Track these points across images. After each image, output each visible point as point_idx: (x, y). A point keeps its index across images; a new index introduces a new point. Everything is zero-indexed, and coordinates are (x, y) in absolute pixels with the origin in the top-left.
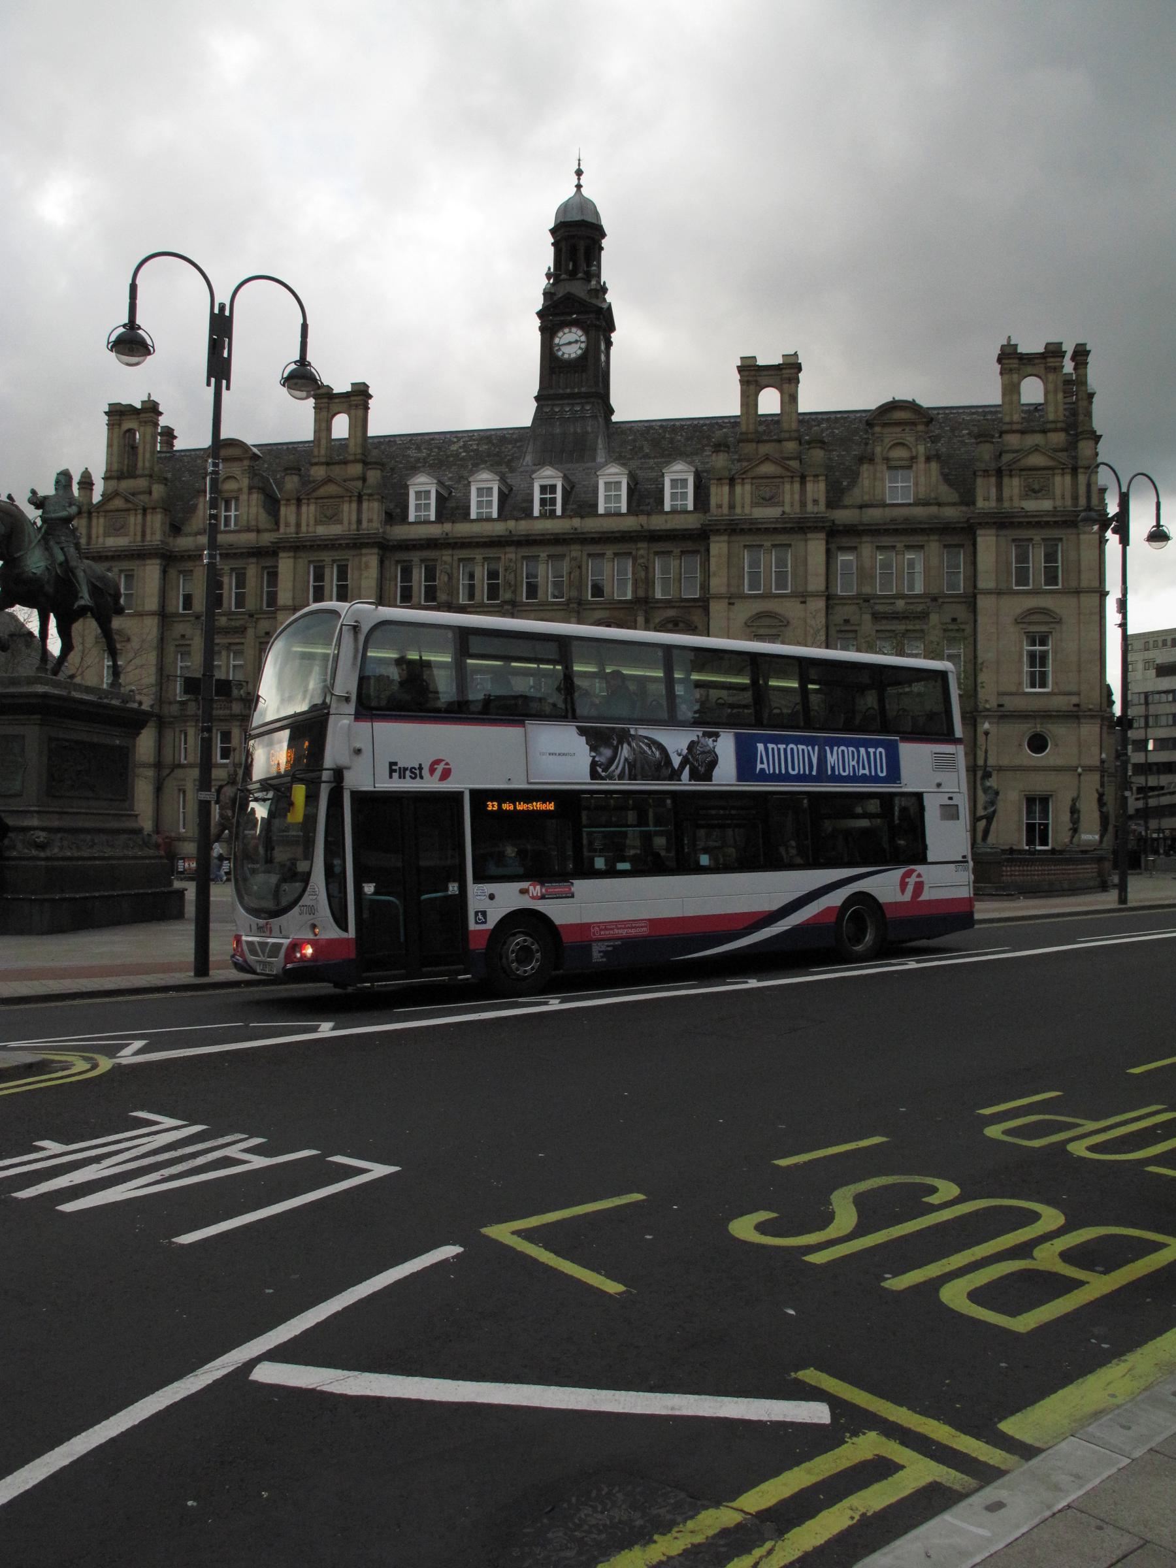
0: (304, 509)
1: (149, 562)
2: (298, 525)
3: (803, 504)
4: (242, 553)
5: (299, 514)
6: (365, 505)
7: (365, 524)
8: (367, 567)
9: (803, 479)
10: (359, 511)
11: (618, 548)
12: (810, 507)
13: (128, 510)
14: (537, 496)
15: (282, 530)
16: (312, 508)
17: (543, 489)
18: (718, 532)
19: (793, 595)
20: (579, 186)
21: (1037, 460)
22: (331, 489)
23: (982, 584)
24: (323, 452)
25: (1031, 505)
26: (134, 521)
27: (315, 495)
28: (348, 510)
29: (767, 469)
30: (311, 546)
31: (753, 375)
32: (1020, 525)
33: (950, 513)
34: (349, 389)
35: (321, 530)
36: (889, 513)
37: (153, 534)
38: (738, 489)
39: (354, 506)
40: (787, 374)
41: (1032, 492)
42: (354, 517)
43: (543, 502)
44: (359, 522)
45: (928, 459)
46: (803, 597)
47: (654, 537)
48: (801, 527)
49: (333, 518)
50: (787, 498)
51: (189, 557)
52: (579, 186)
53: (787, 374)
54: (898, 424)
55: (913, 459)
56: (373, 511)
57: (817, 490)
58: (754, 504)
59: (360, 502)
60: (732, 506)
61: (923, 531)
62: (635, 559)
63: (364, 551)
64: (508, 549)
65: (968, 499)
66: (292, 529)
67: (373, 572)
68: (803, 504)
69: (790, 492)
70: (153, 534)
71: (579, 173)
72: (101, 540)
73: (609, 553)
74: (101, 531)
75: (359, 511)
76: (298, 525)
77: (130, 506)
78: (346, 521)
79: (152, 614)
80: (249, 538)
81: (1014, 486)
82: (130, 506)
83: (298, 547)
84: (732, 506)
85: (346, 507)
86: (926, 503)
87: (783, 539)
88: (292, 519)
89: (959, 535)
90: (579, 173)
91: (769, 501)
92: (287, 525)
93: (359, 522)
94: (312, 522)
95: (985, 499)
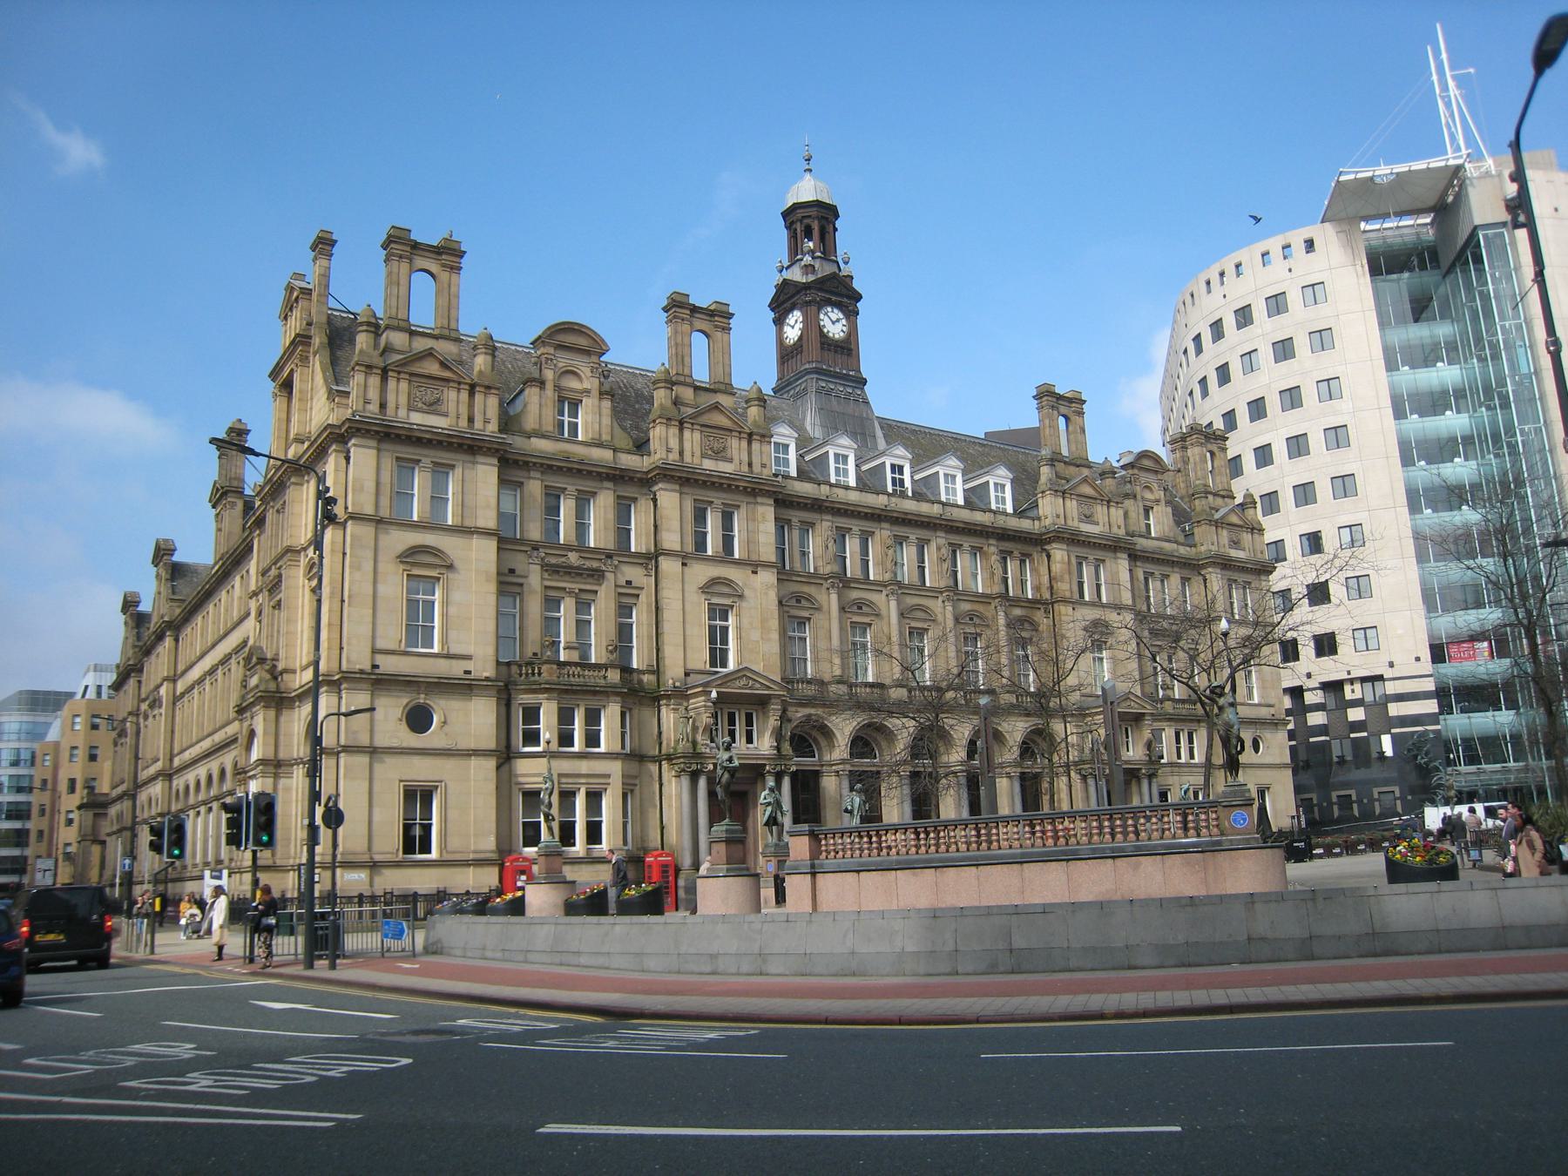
0: (687, 434)
1: (480, 459)
2: (681, 453)
4: (599, 474)
8: (764, 519)
13: (447, 380)
14: (889, 475)
26: (454, 399)
27: (705, 419)
30: (705, 482)
37: (486, 421)
38: (1068, 502)
39: (744, 444)
43: (894, 479)
48: (1113, 546)
49: (719, 454)
51: (526, 463)
58: (1081, 521)
63: (759, 500)
64: (884, 525)
67: (770, 526)
70: (486, 421)
72: (402, 413)
74: (403, 400)
76: (681, 453)
77: (447, 374)
78: (736, 458)
79: (486, 533)
80: (605, 455)
82: (447, 374)
83: (684, 478)
94: (698, 453)
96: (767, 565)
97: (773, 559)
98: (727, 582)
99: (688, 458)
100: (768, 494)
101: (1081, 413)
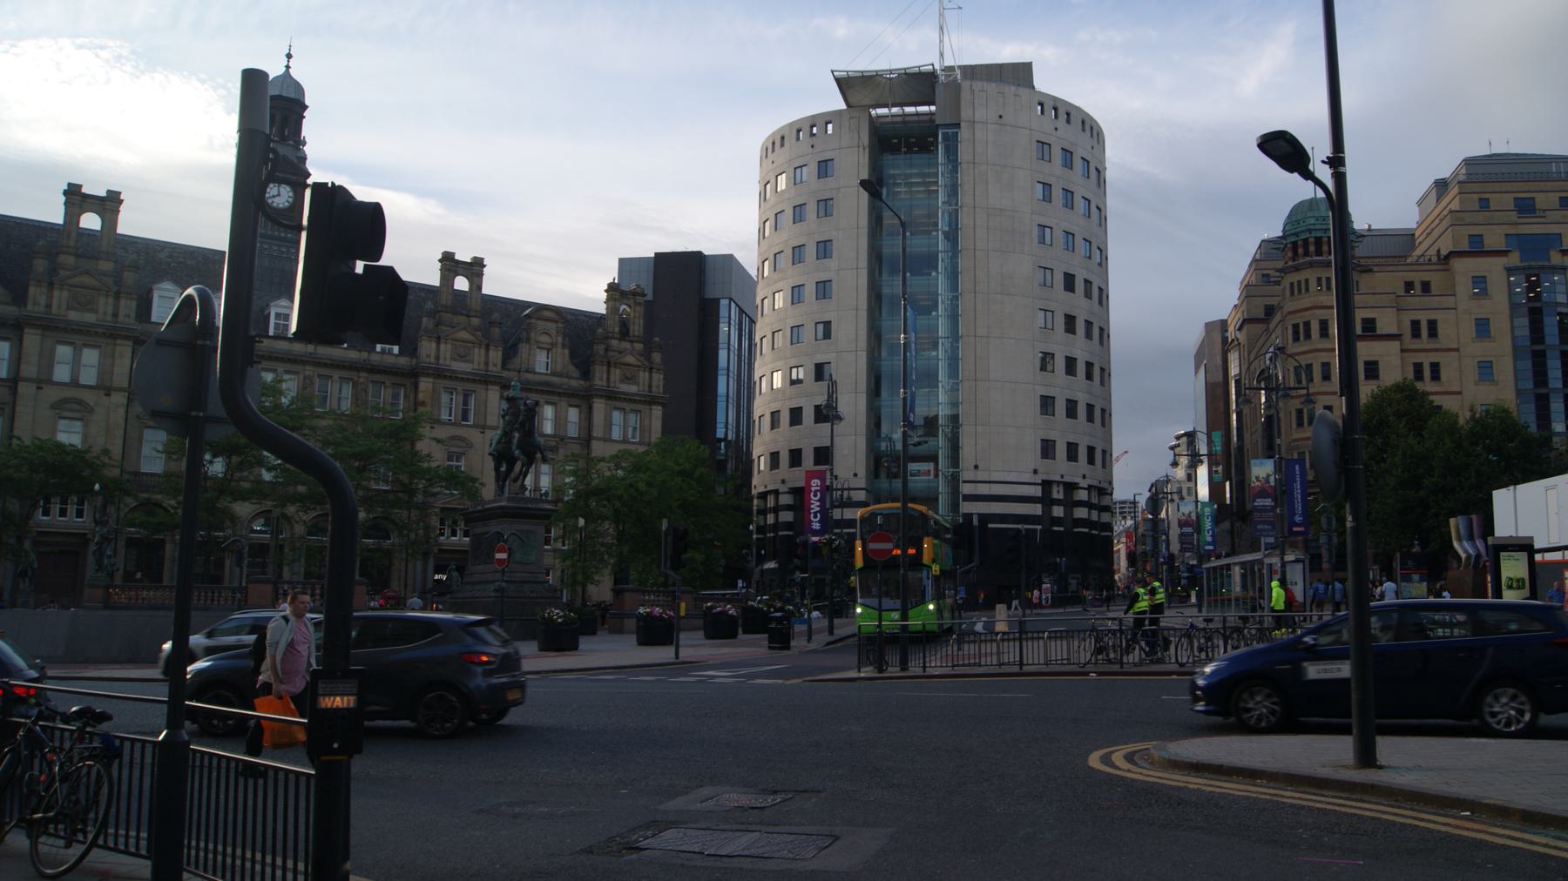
0: (56, 293)
3: (487, 364)
5: (50, 297)
6: (123, 302)
7: (121, 318)
9: (487, 347)
10: (116, 306)
11: (345, 373)
12: (491, 368)
15: (30, 307)
16: (65, 294)
17: (278, 316)
18: (428, 375)
19: (475, 426)
20: (288, 67)
21: (630, 359)
22: (86, 280)
23: (595, 434)
24: (72, 243)
25: (624, 388)
28: (105, 304)
29: (463, 335)
31: (450, 264)
32: (620, 399)
33: (574, 383)
34: (103, 194)
35: (73, 316)
36: (537, 378)
38: (442, 346)
39: (111, 300)
40: (475, 269)
41: (628, 379)
42: (110, 310)
43: (277, 326)
44: (115, 315)
45: (564, 346)
46: (483, 428)
47: (373, 370)
50: (476, 358)
52: (288, 67)
53: (475, 269)
54: (547, 320)
55: (554, 345)
56: (128, 307)
57: (496, 355)
58: (453, 359)
59: (117, 296)
60: (437, 358)
61: (559, 394)
62: (355, 384)
65: (586, 374)
66: (42, 309)
68: (487, 364)
69: (478, 354)
71: (289, 56)
73: (336, 377)
75: (116, 306)
81: (616, 373)
84: (437, 358)
85: (102, 300)
86: (560, 375)
87: (469, 386)
88: (43, 300)
89: (583, 399)
90: (289, 56)
91: (462, 357)
92: (35, 304)
93: (115, 315)
95: (599, 377)
96: (121, 390)
97: (126, 385)
98: (80, 402)
99: (54, 310)
100: (126, 338)
101: (481, 275)
